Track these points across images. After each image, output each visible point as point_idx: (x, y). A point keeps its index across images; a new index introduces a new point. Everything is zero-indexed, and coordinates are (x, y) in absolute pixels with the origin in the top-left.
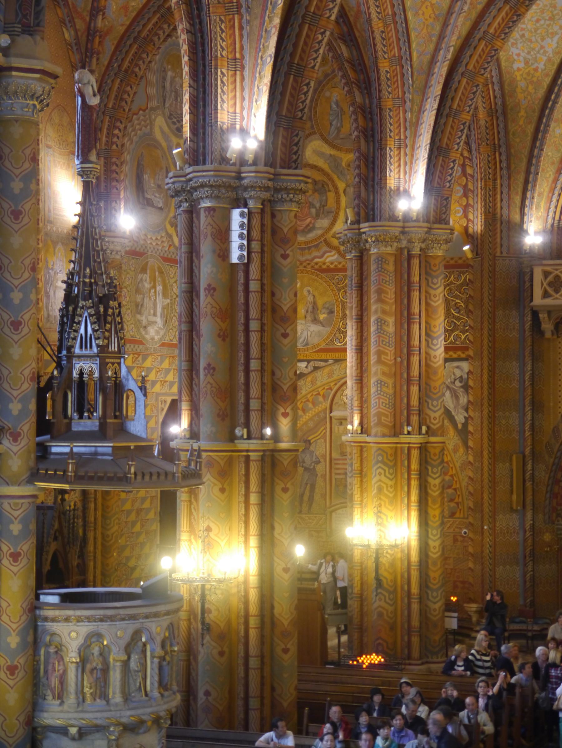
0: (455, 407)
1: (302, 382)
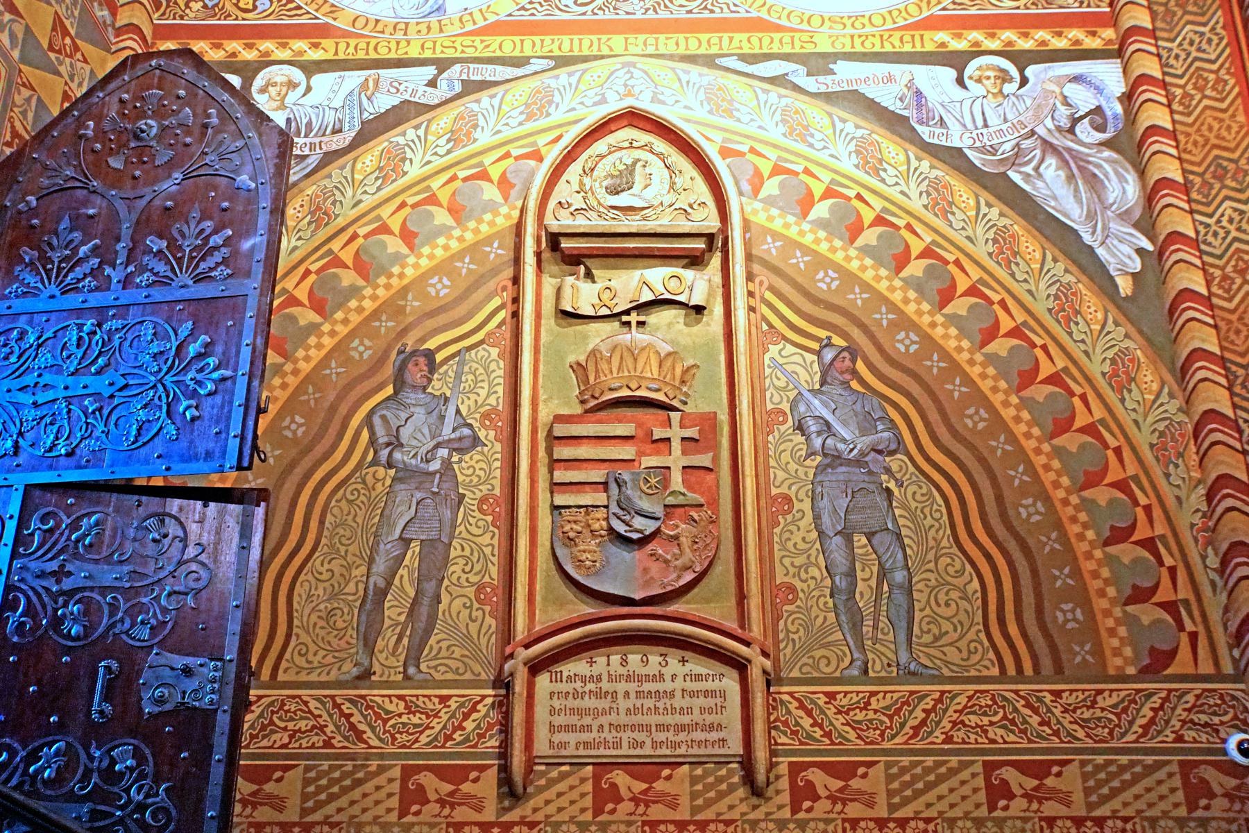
0: (1091, 216)
1: (411, 134)
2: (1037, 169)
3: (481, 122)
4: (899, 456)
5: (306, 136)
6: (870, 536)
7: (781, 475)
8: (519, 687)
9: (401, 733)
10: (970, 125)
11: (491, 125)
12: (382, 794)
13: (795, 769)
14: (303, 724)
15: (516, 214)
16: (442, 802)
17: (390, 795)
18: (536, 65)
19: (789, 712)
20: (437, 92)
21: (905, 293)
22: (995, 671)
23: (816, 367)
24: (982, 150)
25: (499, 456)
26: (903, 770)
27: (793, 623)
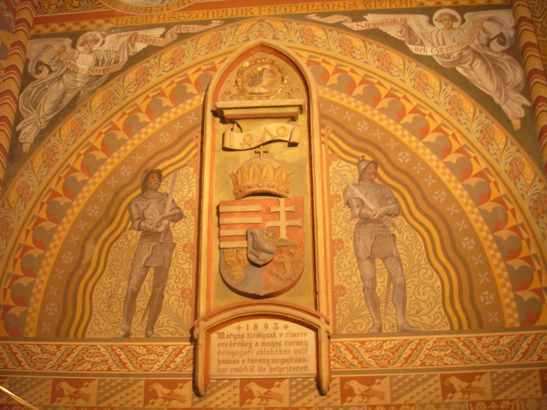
0: (499, 89)
1: (152, 61)
2: (471, 65)
3: (187, 54)
4: (400, 217)
5: (102, 66)
6: (384, 259)
7: (338, 229)
8: (202, 341)
9: (145, 364)
10: (436, 44)
11: (191, 54)
12: (135, 394)
13: (343, 381)
14: (97, 359)
15: (202, 99)
16: (165, 398)
17: (139, 394)
18: (214, 24)
19: (340, 352)
20: (165, 40)
21: (403, 131)
22: (448, 328)
23: (356, 172)
24: (443, 56)
25: (193, 223)
26: (399, 380)
27: (343, 305)
